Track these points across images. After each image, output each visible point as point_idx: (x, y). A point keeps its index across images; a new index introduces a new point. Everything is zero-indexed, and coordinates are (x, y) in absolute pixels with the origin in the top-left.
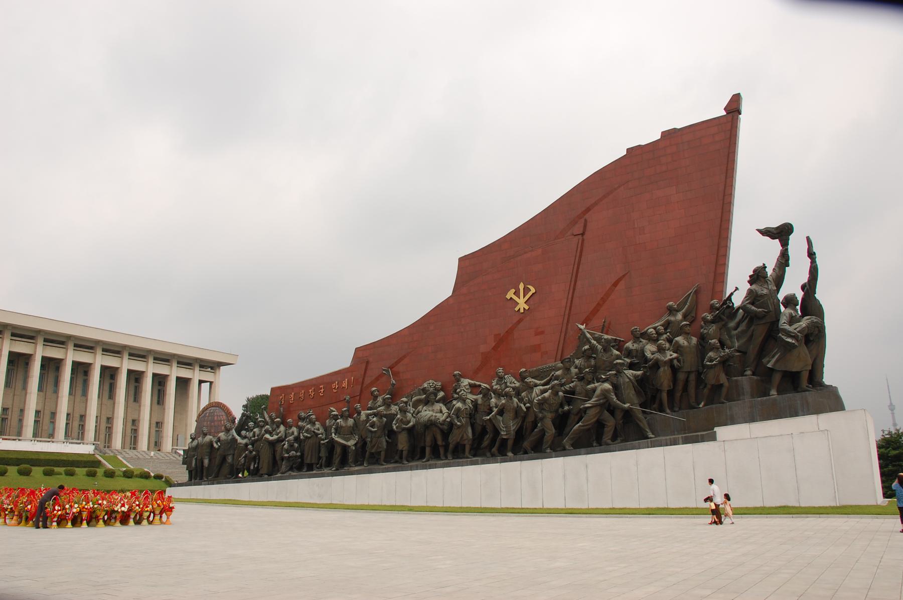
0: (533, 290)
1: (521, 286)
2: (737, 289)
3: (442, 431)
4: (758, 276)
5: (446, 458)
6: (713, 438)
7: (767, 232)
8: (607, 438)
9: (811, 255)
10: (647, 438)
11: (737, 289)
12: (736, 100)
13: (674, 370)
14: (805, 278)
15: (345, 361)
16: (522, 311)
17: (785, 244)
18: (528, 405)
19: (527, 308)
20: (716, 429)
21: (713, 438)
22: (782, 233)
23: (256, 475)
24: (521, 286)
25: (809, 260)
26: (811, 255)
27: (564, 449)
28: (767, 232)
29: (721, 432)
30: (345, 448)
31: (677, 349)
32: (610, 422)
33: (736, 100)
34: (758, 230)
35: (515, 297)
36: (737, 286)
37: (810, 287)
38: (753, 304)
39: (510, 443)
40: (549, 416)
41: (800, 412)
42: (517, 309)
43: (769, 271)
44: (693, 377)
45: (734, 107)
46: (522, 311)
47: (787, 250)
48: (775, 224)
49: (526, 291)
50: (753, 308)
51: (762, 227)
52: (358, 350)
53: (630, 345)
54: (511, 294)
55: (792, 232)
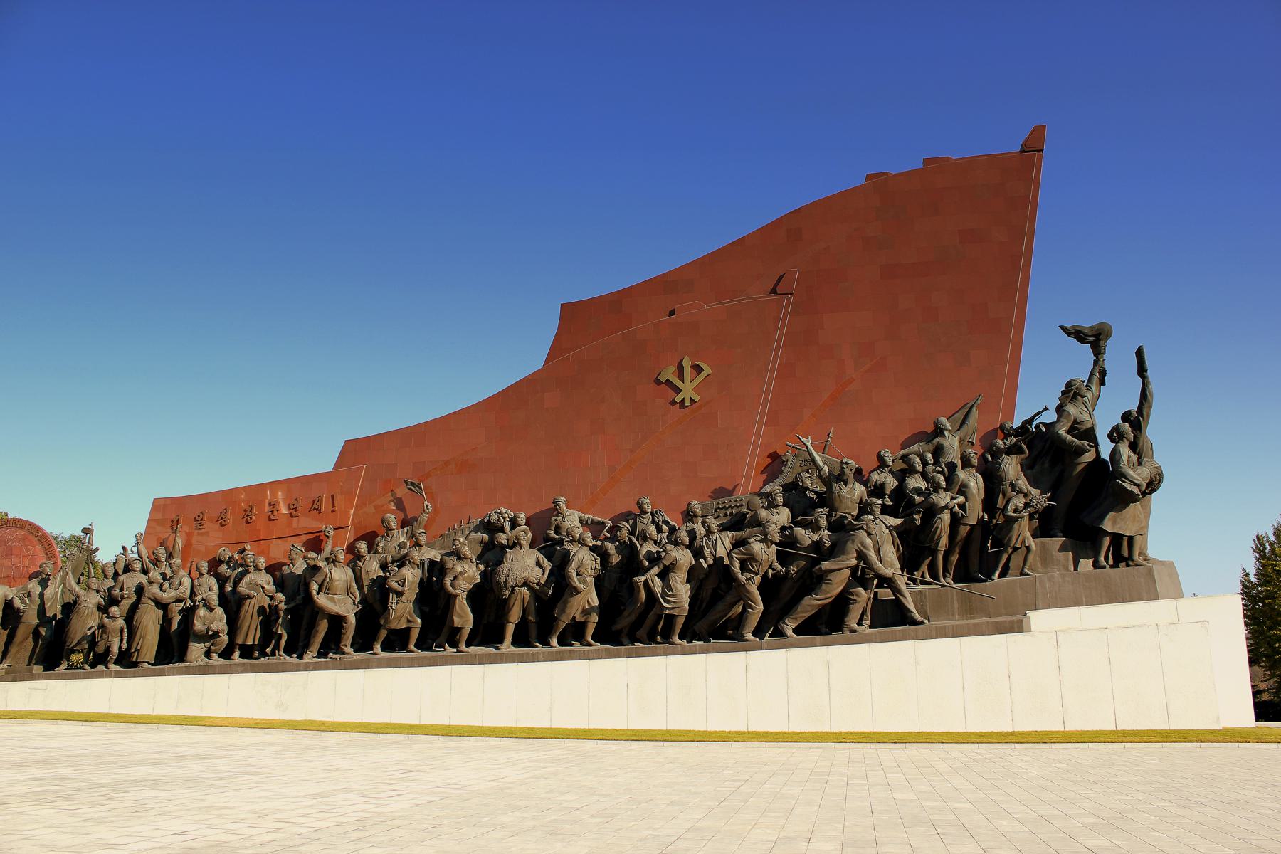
2: (1046, 409)
4: (1071, 393)
5: (546, 643)
8: (852, 621)
9: (1142, 371)
10: (915, 622)
11: (1046, 409)
12: (1038, 132)
13: (956, 520)
17: (1098, 351)
19: (697, 398)
24: (687, 363)
26: (1142, 371)
28: (1078, 334)
29: (1038, 618)
30: (337, 622)
31: (963, 490)
33: (1038, 132)
37: (1135, 420)
38: (1068, 432)
39: (680, 622)
40: (758, 579)
41: (1040, 604)
42: (678, 399)
46: (687, 403)
48: (1087, 322)
50: (1069, 437)
51: (1068, 325)
53: (876, 477)
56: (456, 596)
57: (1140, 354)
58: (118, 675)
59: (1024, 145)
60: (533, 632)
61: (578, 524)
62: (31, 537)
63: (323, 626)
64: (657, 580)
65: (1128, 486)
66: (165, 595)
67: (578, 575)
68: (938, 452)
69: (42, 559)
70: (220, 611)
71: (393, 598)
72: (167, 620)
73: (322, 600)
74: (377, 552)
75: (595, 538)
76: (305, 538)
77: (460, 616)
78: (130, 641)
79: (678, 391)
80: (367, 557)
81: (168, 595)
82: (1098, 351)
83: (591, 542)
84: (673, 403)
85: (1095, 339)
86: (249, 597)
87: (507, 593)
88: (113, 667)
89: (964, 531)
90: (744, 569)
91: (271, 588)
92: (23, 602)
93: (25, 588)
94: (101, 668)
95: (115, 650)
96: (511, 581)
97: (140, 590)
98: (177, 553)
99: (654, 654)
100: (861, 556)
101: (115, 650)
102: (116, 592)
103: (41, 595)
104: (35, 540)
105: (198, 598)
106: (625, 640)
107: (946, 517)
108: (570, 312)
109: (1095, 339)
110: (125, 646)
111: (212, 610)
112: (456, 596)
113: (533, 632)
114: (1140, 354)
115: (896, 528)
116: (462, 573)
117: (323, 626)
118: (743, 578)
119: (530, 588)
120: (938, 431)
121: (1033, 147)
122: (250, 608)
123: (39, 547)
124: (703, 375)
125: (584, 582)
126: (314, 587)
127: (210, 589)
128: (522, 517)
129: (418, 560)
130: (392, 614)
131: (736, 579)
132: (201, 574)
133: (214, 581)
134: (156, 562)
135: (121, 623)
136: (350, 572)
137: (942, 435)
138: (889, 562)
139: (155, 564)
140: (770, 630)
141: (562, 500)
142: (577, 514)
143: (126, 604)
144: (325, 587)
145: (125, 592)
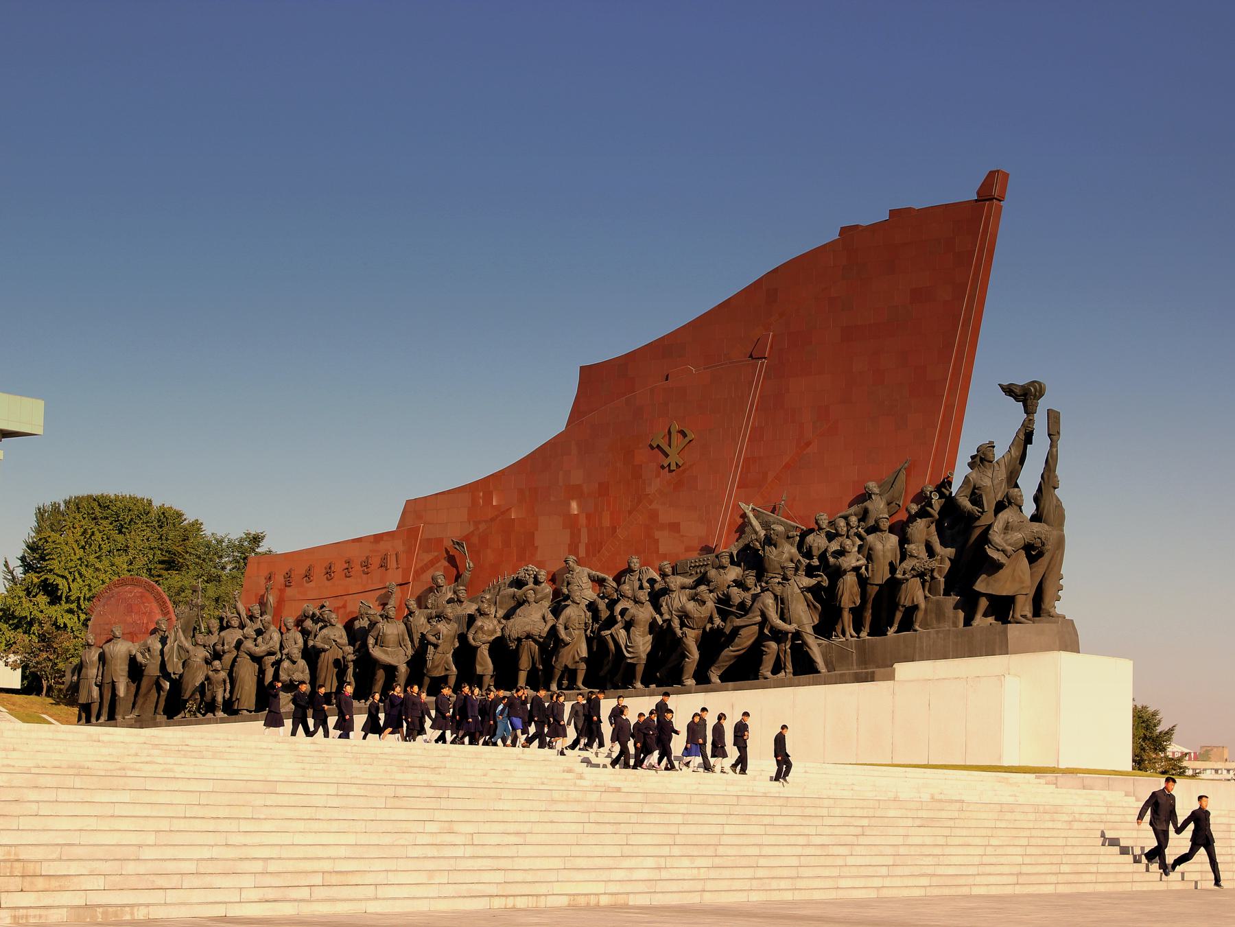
4: (981, 459)
6: (891, 677)
7: (1009, 390)
8: (766, 670)
17: (1029, 410)
18: (667, 617)
20: (896, 665)
21: (891, 677)
22: (1026, 395)
28: (1009, 390)
29: (902, 669)
39: (640, 670)
43: (999, 453)
45: (990, 192)
46: (673, 467)
47: (1031, 421)
48: (1021, 380)
55: (1041, 395)
56: (476, 648)
58: (223, 721)
59: (978, 193)
61: (585, 579)
62: (147, 594)
63: (381, 675)
64: (623, 632)
65: (991, 553)
66: (257, 649)
67: (566, 628)
68: (864, 515)
69: (158, 616)
70: (302, 663)
71: (431, 649)
72: (262, 672)
73: (376, 652)
74: (426, 608)
76: (378, 593)
77: (481, 665)
78: (231, 692)
79: (667, 455)
80: (417, 613)
81: (260, 650)
82: (1029, 410)
84: (663, 467)
85: (1026, 395)
86: (324, 650)
87: (513, 646)
88: (220, 714)
89: (873, 591)
90: (682, 625)
91: (345, 640)
92: (144, 657)
93: (145, 644)
94: (210, 715)
95: (220, 699)
96: (514, 635)
97: (239, 644)
98: (270, 610)
100: (763, 614)
101: (220, 699)
102: (219, 648)
103: (162, 652)
104: (151, 597)
105: (285, 651)
107: (850, 579)
108: (589, 375)
110: (227, 695)
111: (294, 663)
112: (476, 648)
115: (809, 589)
116: (481, 628)
117: (381, 675)
118: (679, 632)
119: (535, 641)
120: (866, 496)
121: (990, 192)
122: (326, 659)
123: (155, 604)
124: (687, 439)
125: (569, 635)
126: (371, 641)
127: (295, 642)
128: (543, 576)
129: (450, 616)
130: (429, 664)
131: (675, 634)
132: (288, 630)
133: (299, 636)
134: (252, 618)
135: (223, 674)
136: (402, 627)
137: (870, 497)
138: (804, 617)
139: (251, 620)
141: (572, 558)
142: (587, 570)
143: (228, 658)
144: (380, 641)
145: (226, 647)
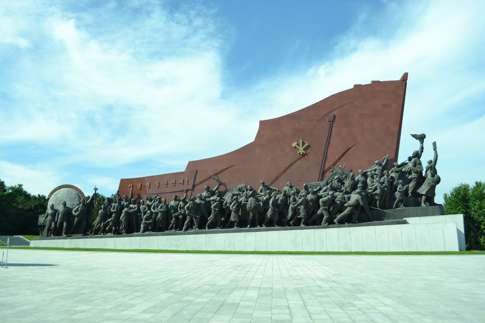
0: (307, 144)
1: (301, 141)
3: (259, 213)
6: (405, 222)
7: (414, 136)
9: (435, 149)
14: (432, 158)
15: (181, 166)
16: (301, 154)
17: (422, 142)
19: (304, 152)
22: (421, 138)
23: (118, 233)
25: (434, 152)
26: (435, 149)
27: (335, 223)
28: (414, 136)
32: (357, 213)
34: (411, 134)
35: (297, 146)
36: (403, 158)
42: (298, 152)
44: (388, 195)
45: (405, 77)
46: (301, 154)
48: (419, 133)
49: (303, 143)
52: (189, 162)
54: (294, 144)
57: (434, 144)
60: (257, 222)
75: (245, 192)
83: (246, 192)
99: (272, 230)
106: (302, 225)
109: (421, 138)
113: (257, 222)
114: (434, 144)
140: (331, 223)
